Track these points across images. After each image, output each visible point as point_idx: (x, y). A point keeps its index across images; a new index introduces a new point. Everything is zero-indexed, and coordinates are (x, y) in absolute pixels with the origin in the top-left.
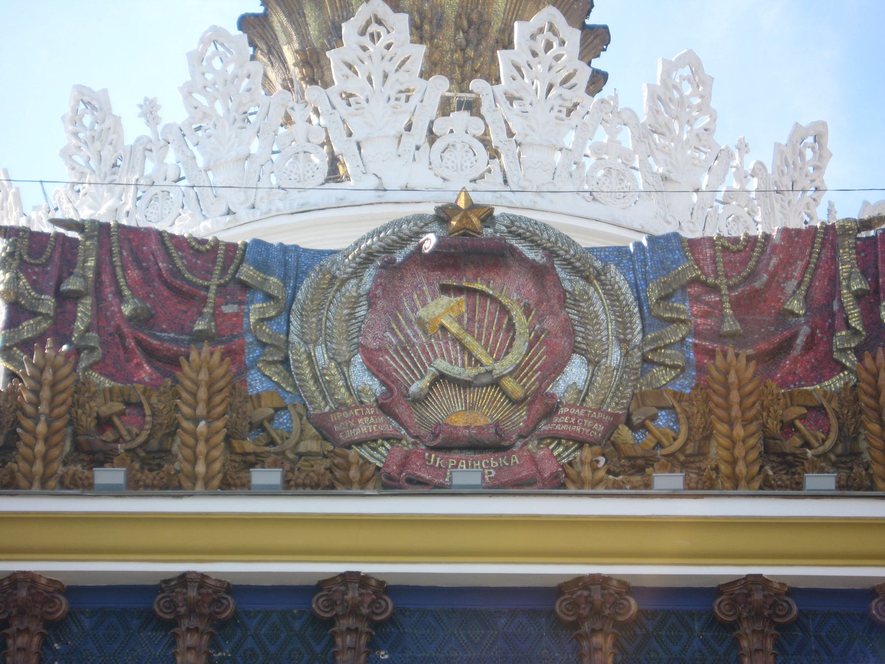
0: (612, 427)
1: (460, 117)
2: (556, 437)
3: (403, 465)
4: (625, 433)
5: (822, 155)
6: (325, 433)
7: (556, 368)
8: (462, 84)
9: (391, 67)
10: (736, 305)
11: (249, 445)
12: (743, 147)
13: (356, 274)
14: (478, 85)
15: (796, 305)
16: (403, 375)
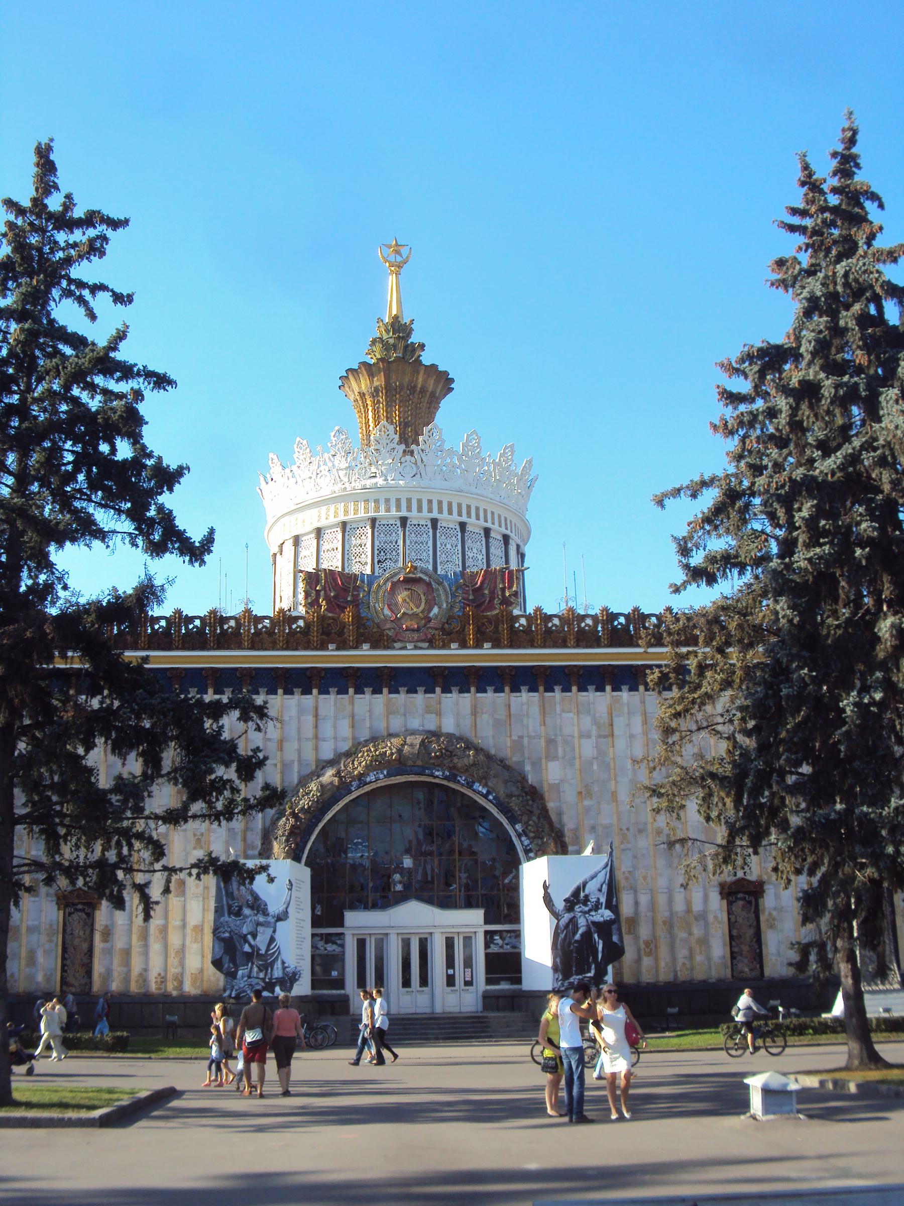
0: (443, 625)
1: (408, 457)
2: (431, 628)
3: (396, 635)
4: (446, 626)
5: (513, 452)
6: (378, 627)
7: (430, 610)
8: (407, 446)
9: (388, 442)
10: (473, 591)
11: (362, 631)
12: (489, 456)
13: (385, 583)
14: (413, 447)
15: (486, 592)
16: (396, 612)
